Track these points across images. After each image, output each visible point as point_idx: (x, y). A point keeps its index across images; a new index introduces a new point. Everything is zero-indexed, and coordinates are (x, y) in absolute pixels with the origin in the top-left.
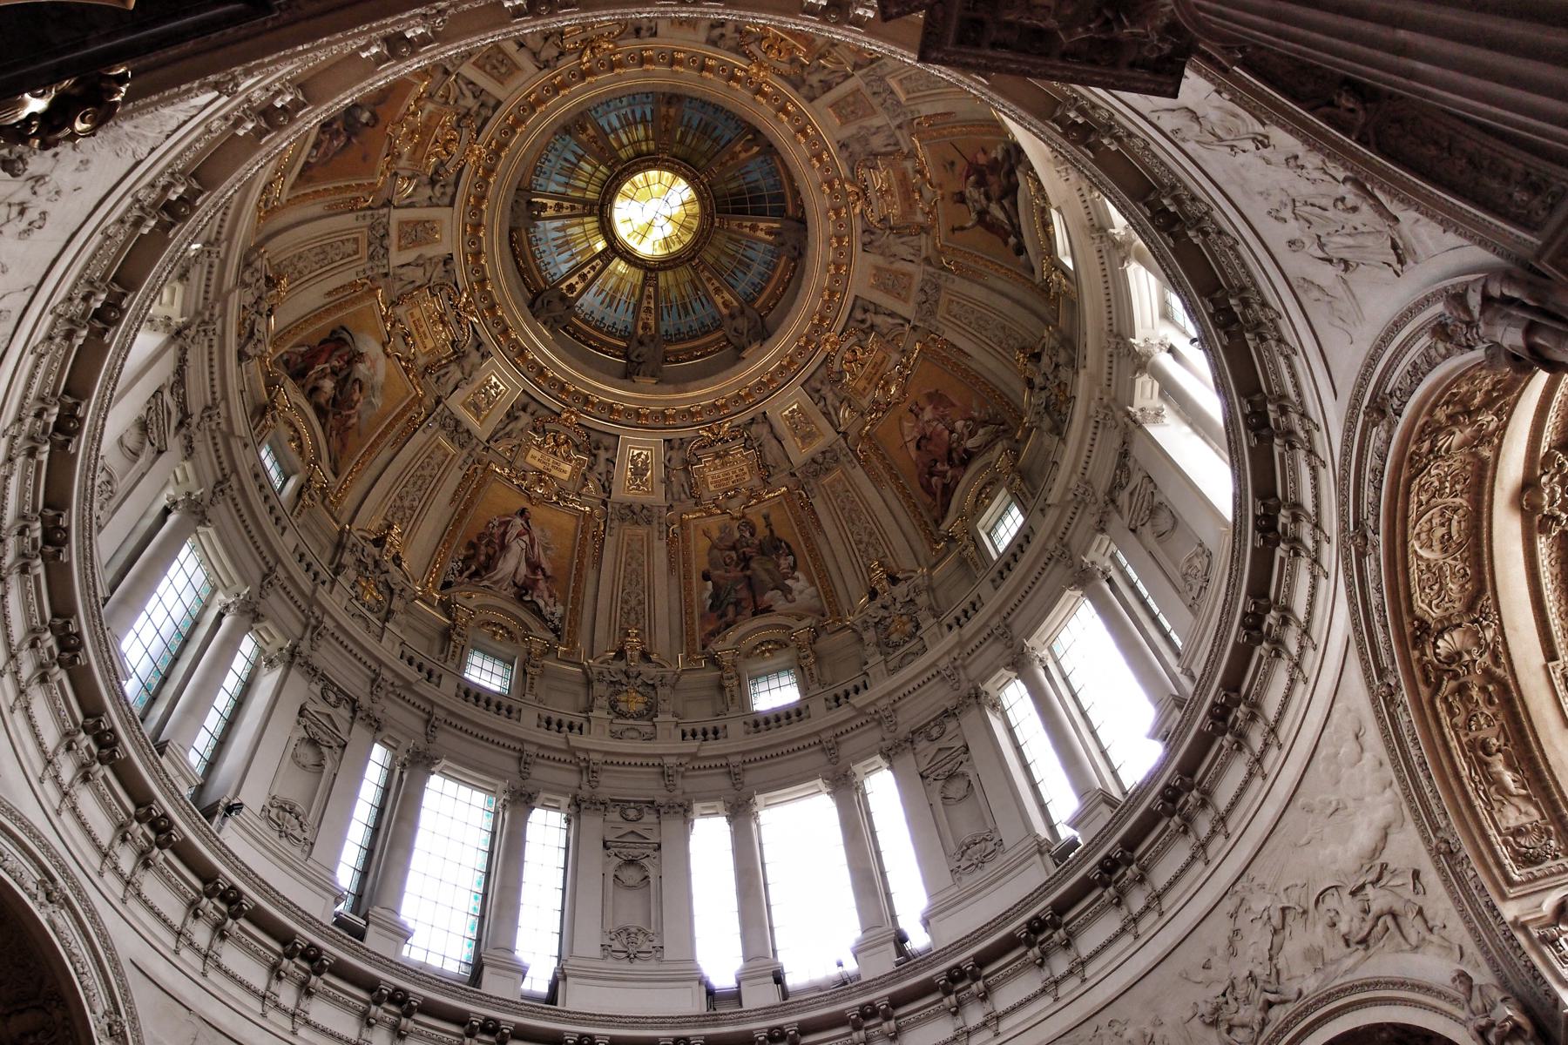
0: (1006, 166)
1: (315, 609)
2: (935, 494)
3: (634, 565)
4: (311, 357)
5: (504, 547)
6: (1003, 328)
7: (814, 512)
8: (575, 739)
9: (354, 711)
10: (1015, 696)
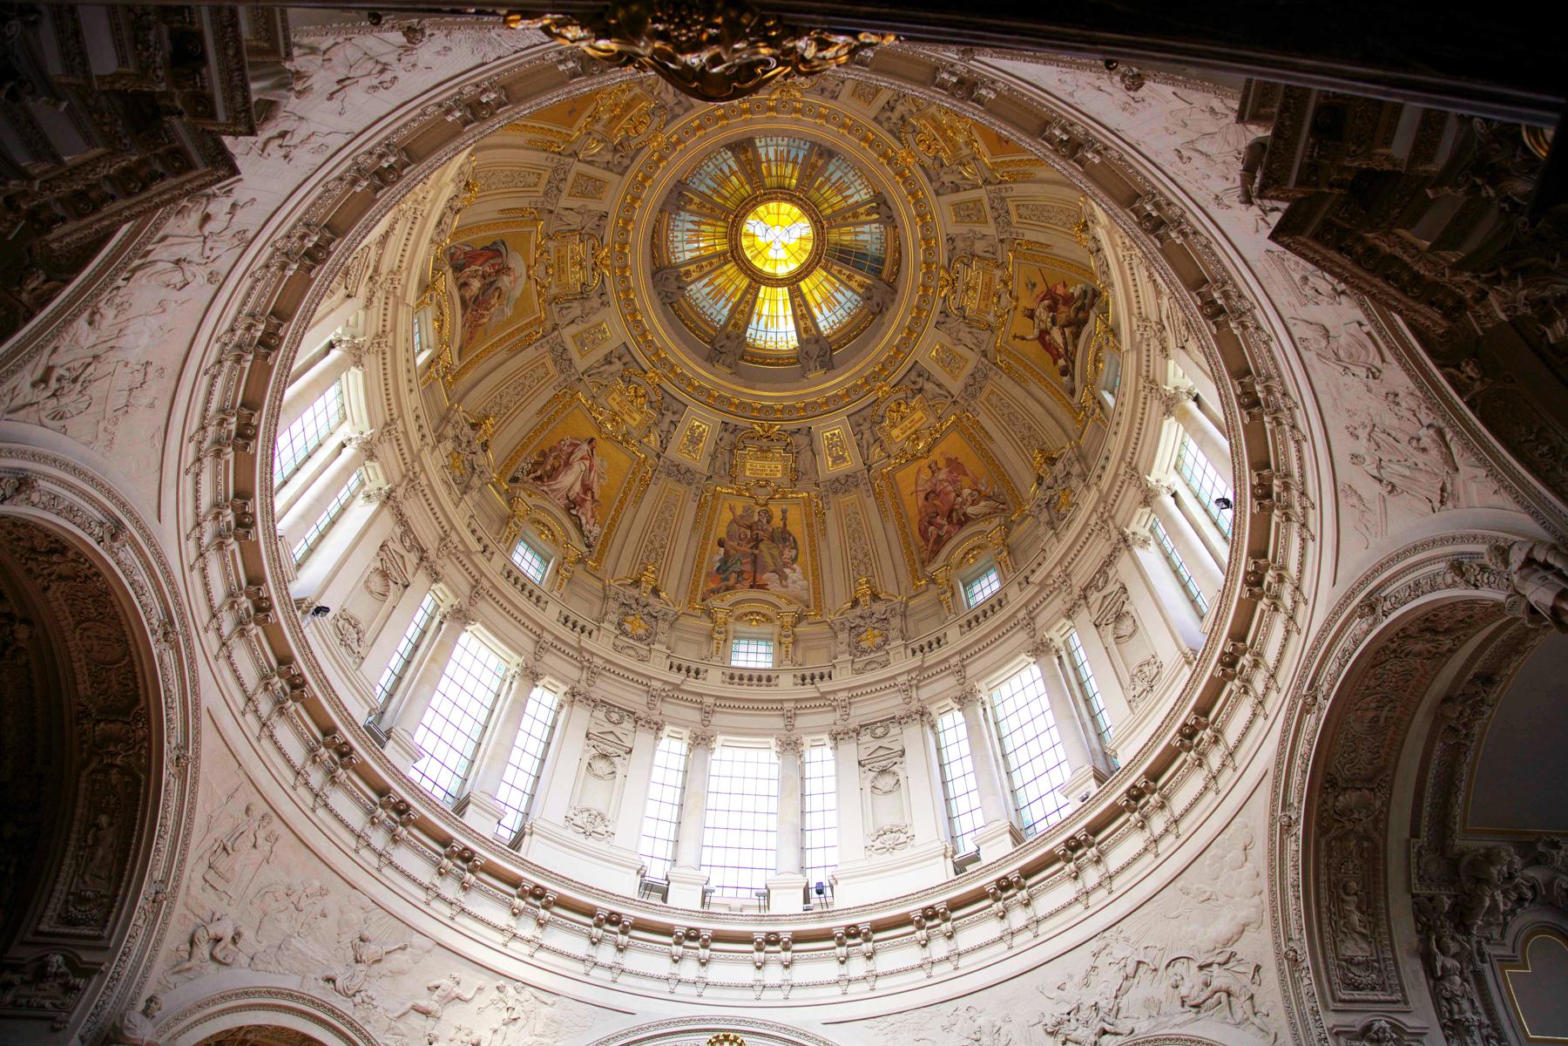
0: (1079, 304)
1: (416, 464)
3: (666, 514)
4: (472, 257)
5: (568, 464)
6: (1030, 428)
7: (824, 522)
8: (586, 642)
9: (421, 559)
10: (952, 723)
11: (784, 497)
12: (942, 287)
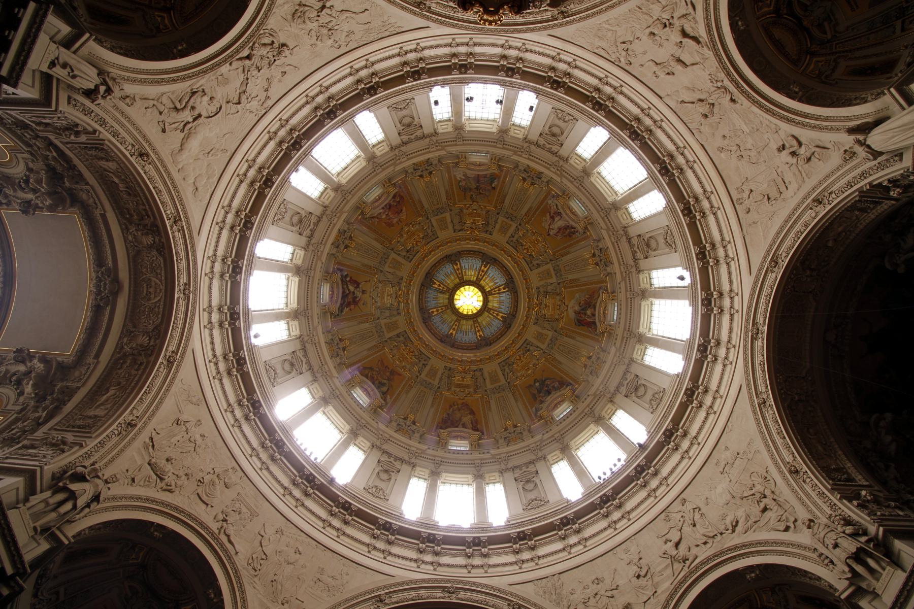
5: (560, 229)
11: (465, 205)
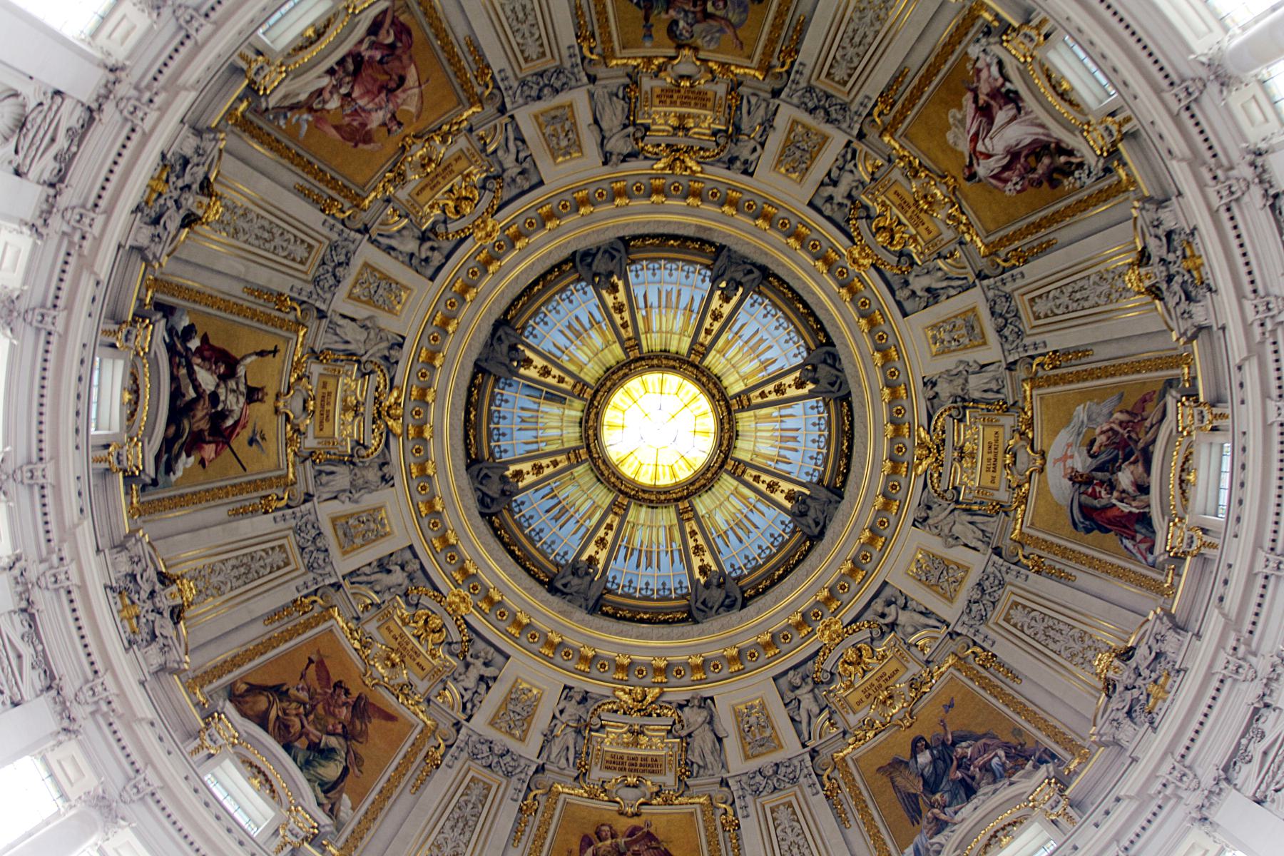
0: (177, 447)
2: (393, 23)
5: (1014, 155)
7: (578, 26)
11: (649, 60)
12: (397, 404)
